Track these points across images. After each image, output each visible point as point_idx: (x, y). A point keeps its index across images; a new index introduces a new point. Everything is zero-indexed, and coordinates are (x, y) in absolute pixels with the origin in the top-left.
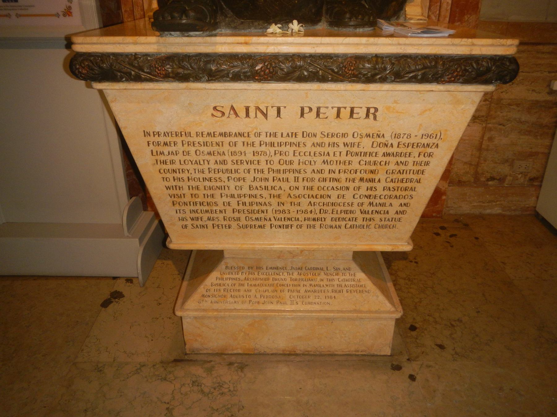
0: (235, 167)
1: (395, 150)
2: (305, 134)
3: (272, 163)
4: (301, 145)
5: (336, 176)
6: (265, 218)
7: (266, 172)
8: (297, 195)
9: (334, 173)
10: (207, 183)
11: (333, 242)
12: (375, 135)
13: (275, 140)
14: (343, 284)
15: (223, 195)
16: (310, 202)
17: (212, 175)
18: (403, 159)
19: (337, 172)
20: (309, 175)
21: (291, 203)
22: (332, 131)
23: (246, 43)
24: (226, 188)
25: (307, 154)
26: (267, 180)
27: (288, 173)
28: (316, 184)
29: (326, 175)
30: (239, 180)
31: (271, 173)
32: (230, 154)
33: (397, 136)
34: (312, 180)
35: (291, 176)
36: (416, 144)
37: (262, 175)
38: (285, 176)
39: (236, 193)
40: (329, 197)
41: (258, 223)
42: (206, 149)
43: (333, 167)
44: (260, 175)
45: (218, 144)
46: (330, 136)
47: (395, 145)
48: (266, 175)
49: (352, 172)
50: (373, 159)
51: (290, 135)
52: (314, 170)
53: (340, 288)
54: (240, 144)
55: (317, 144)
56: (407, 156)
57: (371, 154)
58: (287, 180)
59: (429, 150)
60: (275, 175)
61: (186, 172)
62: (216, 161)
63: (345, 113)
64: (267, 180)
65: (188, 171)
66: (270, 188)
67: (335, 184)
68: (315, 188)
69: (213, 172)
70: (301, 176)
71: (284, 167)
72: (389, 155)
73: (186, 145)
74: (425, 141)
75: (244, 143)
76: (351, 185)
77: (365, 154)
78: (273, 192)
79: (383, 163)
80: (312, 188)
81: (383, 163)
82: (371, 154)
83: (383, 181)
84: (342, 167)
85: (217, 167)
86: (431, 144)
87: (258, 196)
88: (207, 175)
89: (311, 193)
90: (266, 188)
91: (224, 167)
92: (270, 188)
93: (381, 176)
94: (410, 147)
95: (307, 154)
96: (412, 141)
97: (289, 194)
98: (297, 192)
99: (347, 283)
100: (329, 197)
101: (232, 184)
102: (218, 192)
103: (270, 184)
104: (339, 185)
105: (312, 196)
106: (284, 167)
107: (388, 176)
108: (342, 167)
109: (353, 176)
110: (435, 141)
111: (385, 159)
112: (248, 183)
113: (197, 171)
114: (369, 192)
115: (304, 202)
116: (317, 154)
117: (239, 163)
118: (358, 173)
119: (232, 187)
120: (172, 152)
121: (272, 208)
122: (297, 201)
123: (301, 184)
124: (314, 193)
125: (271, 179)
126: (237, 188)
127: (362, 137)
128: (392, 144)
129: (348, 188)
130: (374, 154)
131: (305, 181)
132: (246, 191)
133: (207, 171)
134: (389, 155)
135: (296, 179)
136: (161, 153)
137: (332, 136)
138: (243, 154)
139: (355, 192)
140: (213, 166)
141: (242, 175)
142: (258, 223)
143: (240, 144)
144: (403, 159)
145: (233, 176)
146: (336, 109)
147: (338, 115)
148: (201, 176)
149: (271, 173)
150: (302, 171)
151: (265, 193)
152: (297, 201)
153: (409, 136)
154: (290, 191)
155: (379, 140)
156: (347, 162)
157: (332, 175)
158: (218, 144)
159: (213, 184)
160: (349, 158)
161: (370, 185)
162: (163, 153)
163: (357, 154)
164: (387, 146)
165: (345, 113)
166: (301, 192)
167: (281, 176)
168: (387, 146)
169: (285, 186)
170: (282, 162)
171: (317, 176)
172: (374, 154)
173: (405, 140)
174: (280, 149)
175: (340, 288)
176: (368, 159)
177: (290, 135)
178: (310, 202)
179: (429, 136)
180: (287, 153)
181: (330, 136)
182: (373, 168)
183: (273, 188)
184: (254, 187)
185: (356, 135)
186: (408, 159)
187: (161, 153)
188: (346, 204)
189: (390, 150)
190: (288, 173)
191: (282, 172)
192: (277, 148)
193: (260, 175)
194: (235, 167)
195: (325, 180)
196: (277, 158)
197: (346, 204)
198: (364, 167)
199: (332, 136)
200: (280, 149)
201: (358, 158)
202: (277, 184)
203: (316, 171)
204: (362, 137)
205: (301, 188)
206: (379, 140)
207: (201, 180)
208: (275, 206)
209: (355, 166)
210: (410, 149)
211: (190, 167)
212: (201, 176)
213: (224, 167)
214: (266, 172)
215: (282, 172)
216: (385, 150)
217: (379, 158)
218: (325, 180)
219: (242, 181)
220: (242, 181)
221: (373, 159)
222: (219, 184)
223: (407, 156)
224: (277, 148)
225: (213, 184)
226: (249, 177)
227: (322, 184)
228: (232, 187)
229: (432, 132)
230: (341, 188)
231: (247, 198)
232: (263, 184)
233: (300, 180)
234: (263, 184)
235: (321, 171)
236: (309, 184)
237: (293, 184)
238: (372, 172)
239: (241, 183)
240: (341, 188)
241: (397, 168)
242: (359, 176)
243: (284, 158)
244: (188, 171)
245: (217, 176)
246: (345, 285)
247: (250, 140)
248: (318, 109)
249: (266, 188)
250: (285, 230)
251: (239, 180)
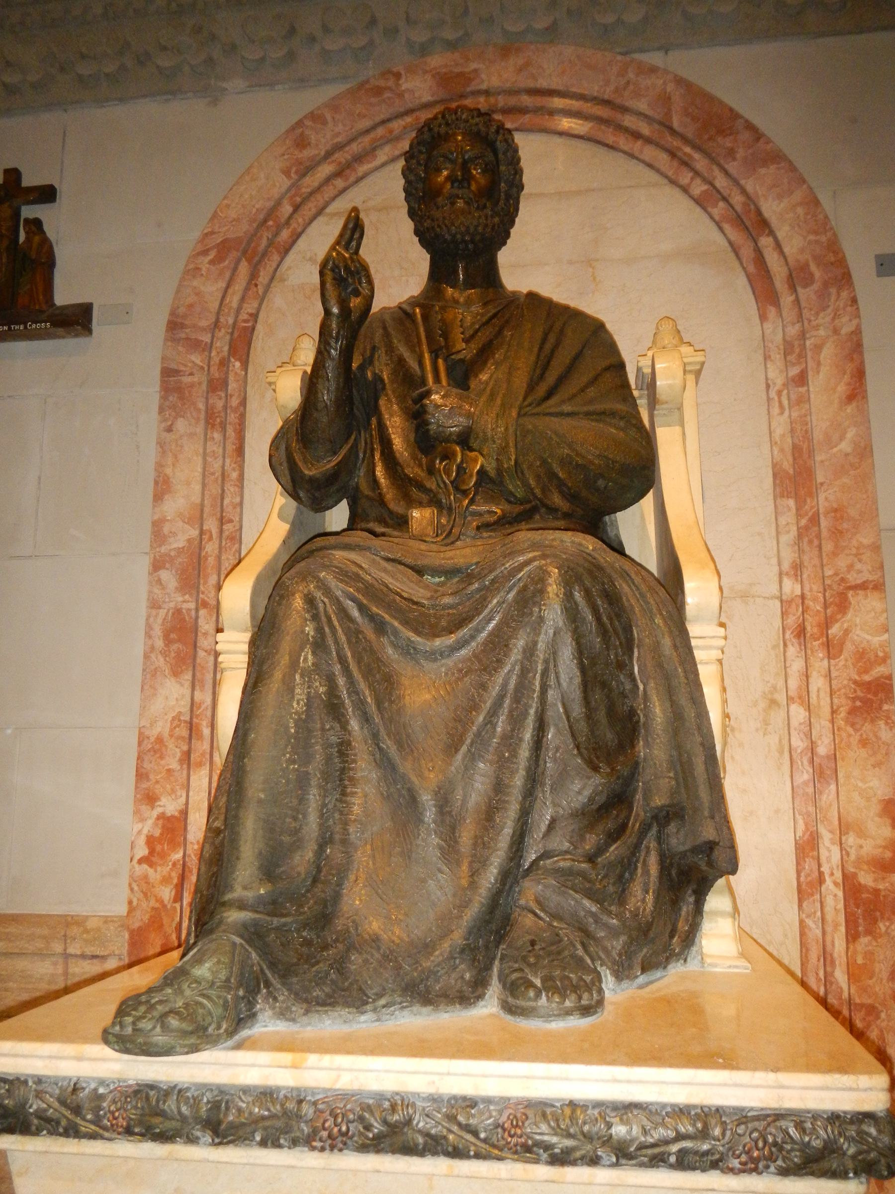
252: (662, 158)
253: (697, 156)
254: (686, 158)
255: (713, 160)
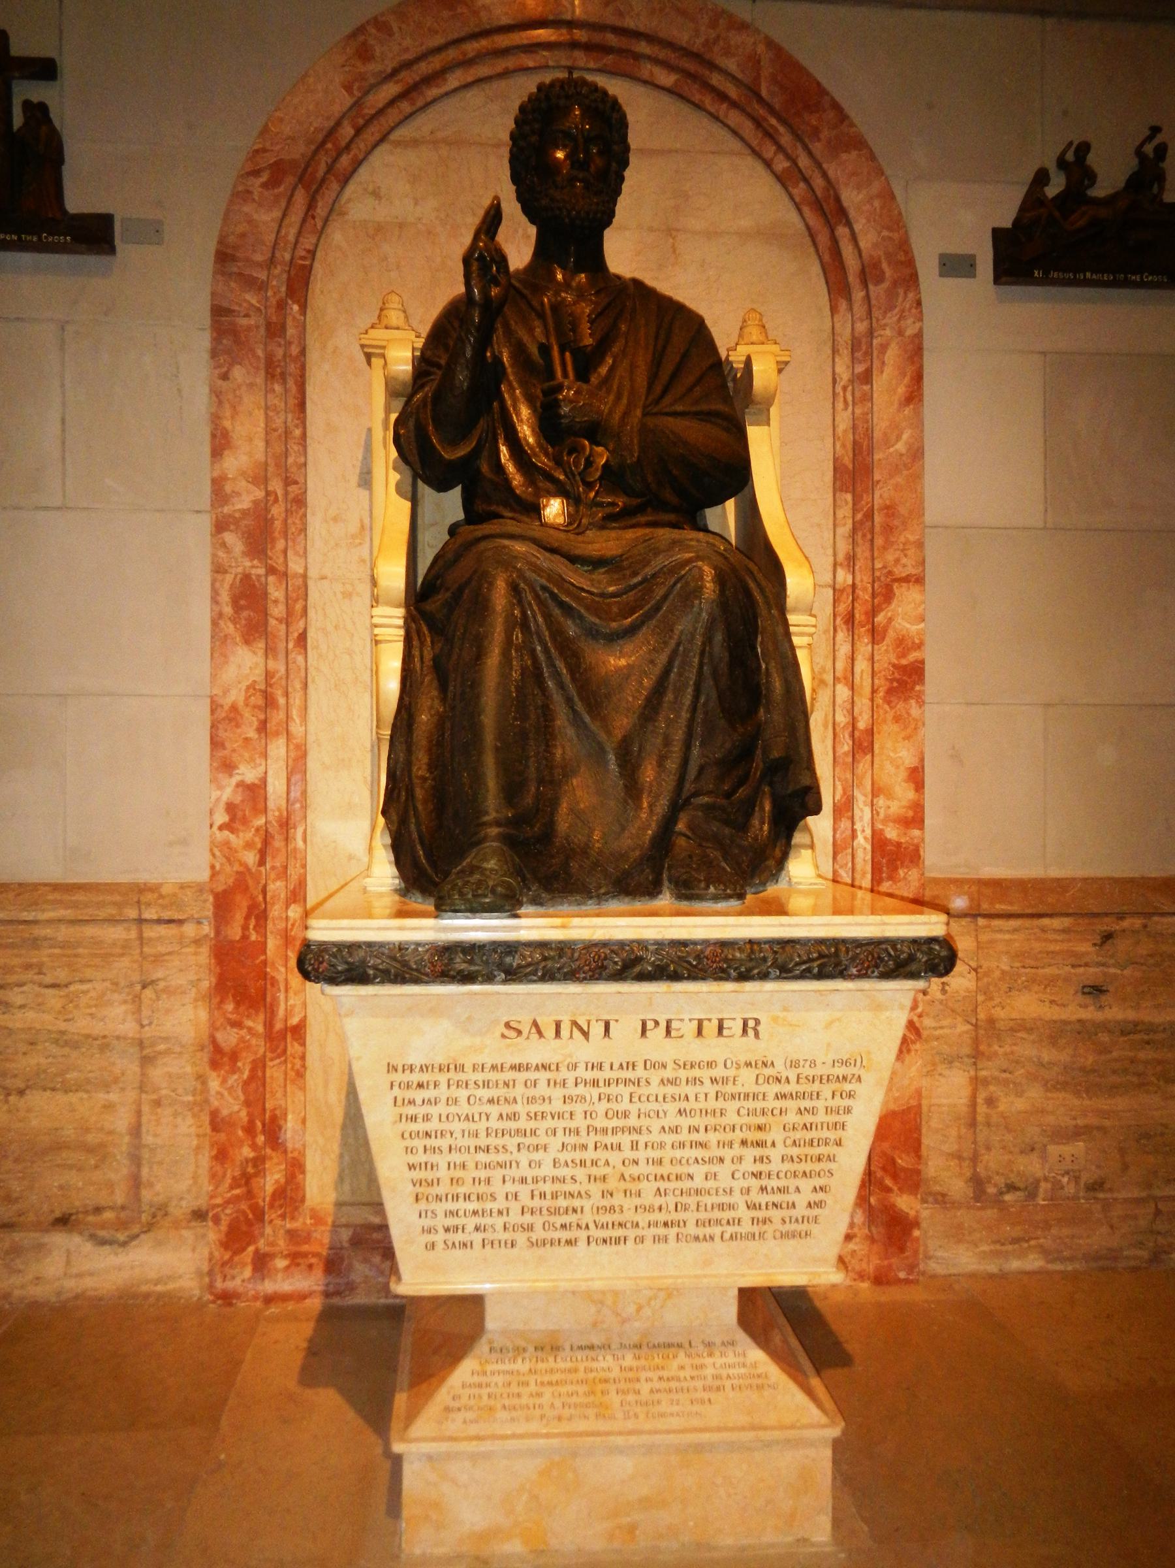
0: (532, 1124)
1: (792, 1088)
2: (648, 1063)
3: (594, 1115)
4: (643, 1083)
5: (700, 1137)
6: (578, 1225)
7: (583, 1133)
8: (636, 1175)
9: (698, 1131)
10: (482, 1157)
11: (699, 1272)
12: (760, 1063)
13: (601, 1075)
14: (724, 1373)
15: (507, 1178)
16: (659, 1189)
17: (492, 1141)
18: (807, 1104)
19: (702, 1129)
20: (655, 1137)
21: (625, 1192)
22: (691, 1058)
23: (564, 927)
24: (514, 1164)
25: (652, 1098)
26: (584, 1147)
27: (619, 1134)
28: (668, 1153)
29: (684, 1136)
30: (537, 1148)
31: (592, 1134)
32: (525, 1101)
33: (795, 1064)
34: (662, 1145)
35: (626, 1139)
36: (825, 1078)
37: (576, 1138)
38: (615, 1139)
39: (529, 1174)
40: (691, 1177)
41: (565, 1235)
42: (485, 1093)
43: (695, 1121)
44: (571, 1140)
45: (506, 1084)
46: (688, 1067)
47: (793, 1079)
48: (583, 1139)
49: (727, 1129)
50: (759, 1105)
51: (625, 1065)
52: (663, 1128)
53: (718, 1383)
54: (542, 1084)
55: (668, 1080)
56: (815, 1097)
57: (755, 1097)
58: (619, 1147)
59: (848, 1087)
60: (599, 1138)
61: (448, 1135)
62: (501, 1115)
63: (710, 1028)
64: (584, 1147)
65: (452, 1134)
66: (588, 1163)
67: (699, 1153)
68: (666, 1161)
69: (493, 1134)
70: (642, 1139)
71: (615, 1123)
72: (784, 1096)
73: (453, 1088)
74: (840, 1071)
75: (549, 1081)
76: (727, 1153)
77: (747, 1096)
78: (595, 1171)
79: (776, 1112)
80: (661, 1162)
81: (776, 1112)
82: (755, 1097)
83: (779, 1144)
84: (710, 1121)
85: (501, 1125)
86: (849, 1077)
87: (568, 1180)
88: (483, 1141)
89: (660, 1170)
90: (583, 1163)
91: (512, 1125)
92: (588, 1163)
93: (776, 1134)
94: (817, 1082)
95: (652, 1098)
96: (820, 1070)
97: (623, 1175)
98: (634, 1170)
99: (731, 1371)
100: (691, 1177)
101: (524, 1158)
102: (497, 1174)
103: (590, 1155)
104: (706, 1154)
105: (662, 1177)
106: (615, 1123)
107: (787, 1134)
108: (710, 1121)
109: (729, 1136)
110: (855, 1071)
111: (778, 1104)
112: (553, 1153)
113: (466, 1134)
114: (758, 1167)
115: (649, 1187)
116: (669, 1099)
117: (539, 1117)
118: (737, 1130)
119: (524, 1163)
120: (429, 1100)
121: (591, 1202)
122: (634, 1187)
123: (641, 1155)
124: (665, 1170)
125: (591, 1146)
126: (533, 1165)
127: (738, 1067)
128: (787, 1078)
129: (721, 1160)
130: (761, 1097)
131: (649, 1148)
132: (547, 1170)
133: (483, 1134)
134: (784, 1096)
135: (634, 1146)
136: (410, 1102)
137: (692, 1066)
138: (547, 1101)
139: (734, 1167)
140: (494, 1124)
141: (542, 1139)
142: (565, 1235)
143: (542, 1084)
144: (807, 1104)
145: (528, 1141)
146: (696, 1022)
147: (700, 1032)
148: (472, 1143)
149: (592, 1134)
150: (644, 1128)
151: (581, 1173)
152: (634, 1187)
153: (813, 1064)
154: (623, 1168)
155: (768, 1071)
156: (718, 1111)
157: (695, 1137)
158: (506, 1084)
159: (492, 1157)
160: (720, 1104)
161: (758, 1152)
162: (414, 1101)
163: (733, 1097)
164: (780, 1081)
165: (710, 1028)
166: (643, 1169)
167: (609, 1139)
168: (780, 1081)
169: (615, 1158)
170: (610, 1114)
171: (669, 1138)
172: (761, 1097)
173: (807, 1071)
174: (607, 1090)
175: (718, 1383)
176: (751, 1104)
177: (625, 1065)
178: (659, 1189)
179: (845, 1063)
180: (619, 1098)
181: (688, 1067)
182: (761, 1120)
183: (594, 1163)
184: (562, 1162)
185: (729, 1065)
186: (814, 1103)
187: (410, 1102)
188: (721, 1191)
189: (786, 1089)
190: (619, 1134)
191: (610, 1132)
192: (602, 1090)
193: (571, 1140)
194: (532, 1124)
195: (682, 1145)
196: (602, 1107)
197: (721, 1191)
198: (745, 1120)
199: (692, 1066)
200: (607, 1090)
201: (735, 1104)
202: (602, 1155)
203: (667, 1129)
204: (738, 1067)
205: (642, 1162)
206: (768, 1071)
207: (472, 1150)
208: (597, 1200)
209: (731, 1118)
210: (816, 1086)
211: (456, 1126)
212: (472, 1143)
213: (512, 1125)
214: (583, 1133)
215: (610, 1132)
216: (776, 1088)
217: (771, 1103)
218: (682, 1145)
219: (541, 1151)
220: (541, 1151)
221: (759, 1105)
222: (501, 1157)
223: (815, 1097)
224: (602, 1090)
225: (492, 1157)
226: (555, 1143)
227: (678, 1153)
228: (524, 1163)
229: (847, 1056)
230: (711, 1161)
231: (549, 1183)
232: (578, 1155)
233: (641, 1145)
234: (578, 1155)
235: (675, 1130)
236: (656, 1154)
237: (628, 1154)
238: (760, 1128)
239: (537, 1156)
240: (711, 1161)
241: (799, 1120)
242: (738, 1135)
243: (614, 1106)
244: (452, 1134)
245: (500, 1142)
246: (729, 1377)
247: (559, 1077)
248: (669, 1022)
249: (583, 1163)
250: (614, 1248)
251: (537, 1148)
252: (747, 128)
253: (781, 129)
254: (771, 131)
255: (798, 137)
